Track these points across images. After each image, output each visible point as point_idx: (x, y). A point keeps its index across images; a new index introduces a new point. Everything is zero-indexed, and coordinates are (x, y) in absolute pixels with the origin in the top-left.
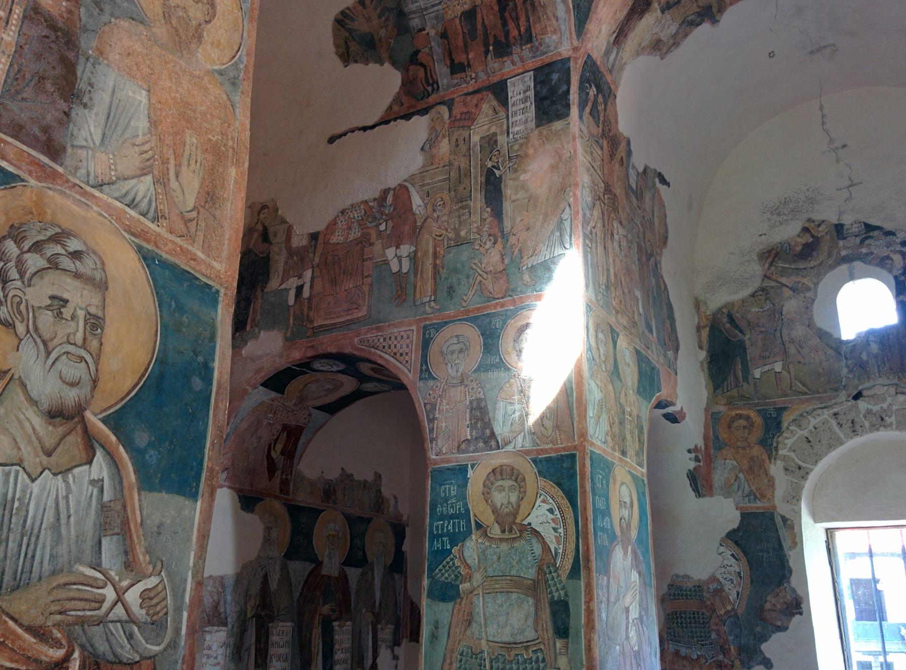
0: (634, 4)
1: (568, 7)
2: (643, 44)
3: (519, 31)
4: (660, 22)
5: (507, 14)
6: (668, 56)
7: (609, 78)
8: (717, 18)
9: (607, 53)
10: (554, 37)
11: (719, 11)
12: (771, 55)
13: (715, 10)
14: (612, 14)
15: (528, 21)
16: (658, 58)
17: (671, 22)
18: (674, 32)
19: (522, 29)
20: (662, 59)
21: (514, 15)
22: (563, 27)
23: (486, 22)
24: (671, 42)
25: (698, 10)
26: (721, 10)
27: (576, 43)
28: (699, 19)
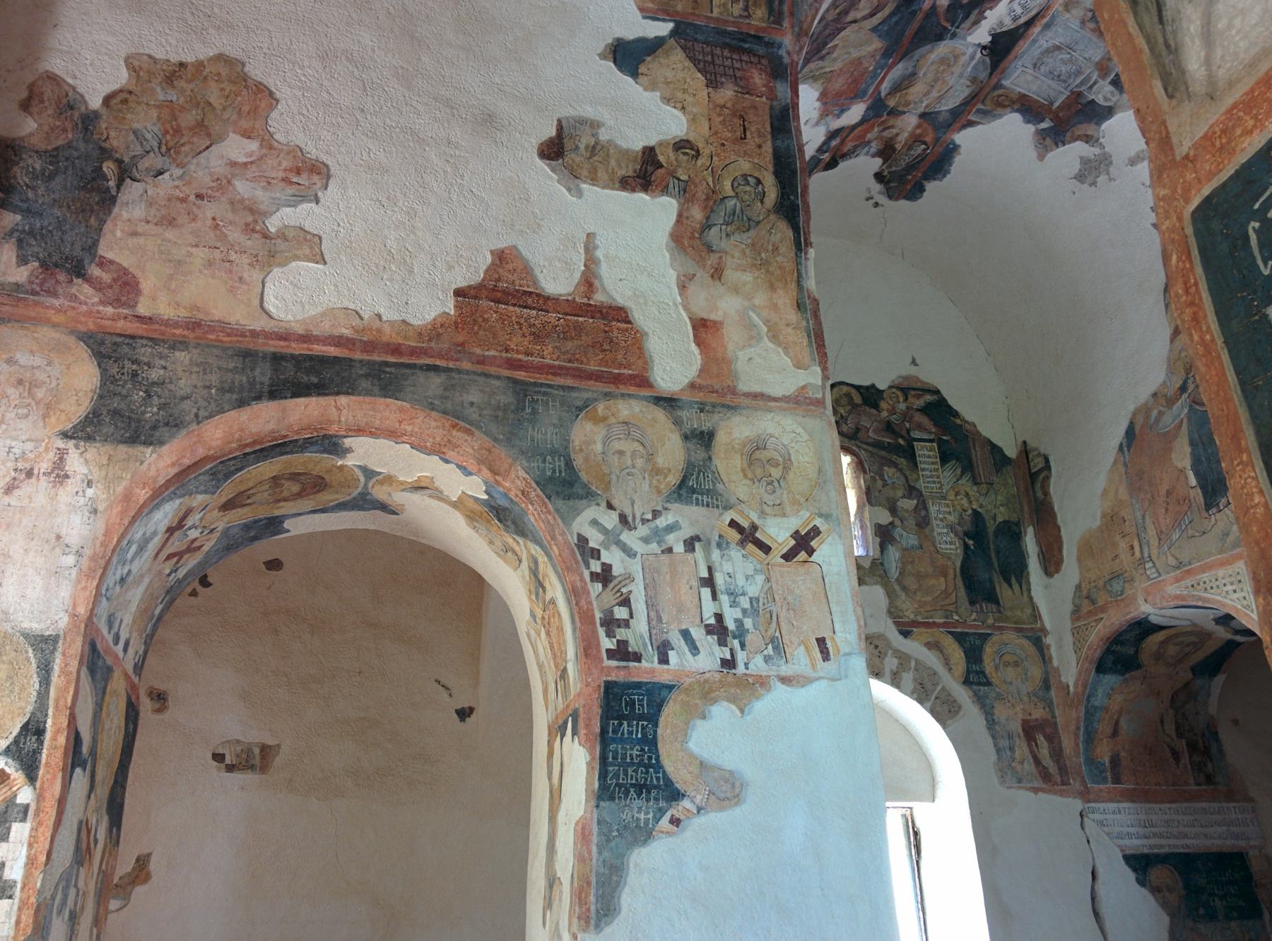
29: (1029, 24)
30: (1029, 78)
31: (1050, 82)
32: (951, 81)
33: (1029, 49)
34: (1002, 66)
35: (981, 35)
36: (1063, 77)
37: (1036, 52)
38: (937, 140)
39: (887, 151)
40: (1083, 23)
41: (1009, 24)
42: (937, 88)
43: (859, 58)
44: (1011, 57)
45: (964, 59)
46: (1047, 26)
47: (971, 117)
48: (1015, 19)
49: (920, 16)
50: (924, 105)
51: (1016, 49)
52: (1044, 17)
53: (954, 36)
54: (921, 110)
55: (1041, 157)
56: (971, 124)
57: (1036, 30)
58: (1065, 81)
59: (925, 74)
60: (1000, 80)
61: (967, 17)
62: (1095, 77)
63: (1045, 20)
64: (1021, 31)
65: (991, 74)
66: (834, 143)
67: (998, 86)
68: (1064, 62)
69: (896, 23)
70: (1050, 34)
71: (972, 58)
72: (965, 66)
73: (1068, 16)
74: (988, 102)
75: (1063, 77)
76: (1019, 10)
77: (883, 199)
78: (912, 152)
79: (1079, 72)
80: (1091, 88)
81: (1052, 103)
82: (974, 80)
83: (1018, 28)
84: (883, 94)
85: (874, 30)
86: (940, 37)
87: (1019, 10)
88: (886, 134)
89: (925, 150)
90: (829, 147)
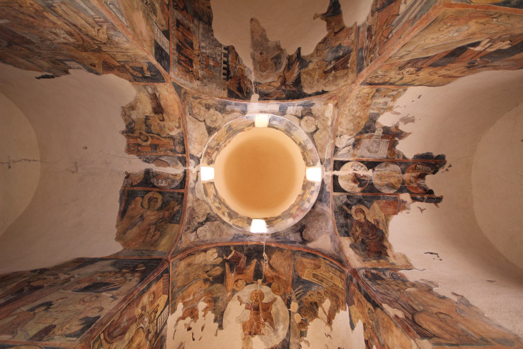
0: (162, 108)
1: (182, 85)
2: (139, 103)
3: (182, 60)
4: (143, 113)
5: (187, 60)
6: (121, 110)
7: (142, 84)
8: (125, 134)
9: (155, 89)
10: (176, 73)
11: (127, 135)
12: (86, 148)
13: (130, 134)
14: (168, 98)
15: (184, 66)
16: (125, 105)
17: (139, 117)
18: (132, 116)
19: (182, 62)
20: (122, 107)
21: (186, 62)
22: (178, 78)
23: (188, 50)
24: (128, 113)
25: (135, 128)
26: (128, 137)
27: (172, 80)
28: (130, 127)
29: (362, 162)
30: (381, 151)
31: (381, 146)
32: (388, 172)
33: (371, 157)
34: (380, 161)
35: (370, 173)
36: (378, 143)
37: (372, 155)
38: (413, 163)
39: (422, 176)
40: (358, 149)
41: (365, 167)
42: (392, 175)
43: (380, 208)
44: (375, 160)
45: (378, 173)
46: (362, 157)
47: (401, 158)
48: (362, 167)
49: (365, 194)
50: (399, 175)
51: (372, 160)
52: (360, 159)
53: (371, 180)
54: (401, 175)
55: (410, 133)
56: (404, 157)
57: (364, 159)
58: (379, 143)
59: (386, 181)
60: (385, 158)
61: (364, 180)
62: (374, 137)
63: (361, 158)
64: (366, 163)
65: (382, 162)
66: (419, 197)
67: (387, 158)
68: (373, 146)
69: (367, 201)
70: (365, 155)
71: (378, 171)
72: (381, 171)
73: (358, 154)
74: (394, 157)
75: (378, 143)
76: (359, 167)
77: (446, 166)
78: (421, 168)
79: (375, 141)
80: (378, 136)
81: (388, 141)
82: (386, 166)
83: (365, 164)
84: (396, 190)
85: (369, 208)
86: (372, 184)
87: (359, 167)
88: (413, 181)
89: (419, 164)
90: (421, 198)
